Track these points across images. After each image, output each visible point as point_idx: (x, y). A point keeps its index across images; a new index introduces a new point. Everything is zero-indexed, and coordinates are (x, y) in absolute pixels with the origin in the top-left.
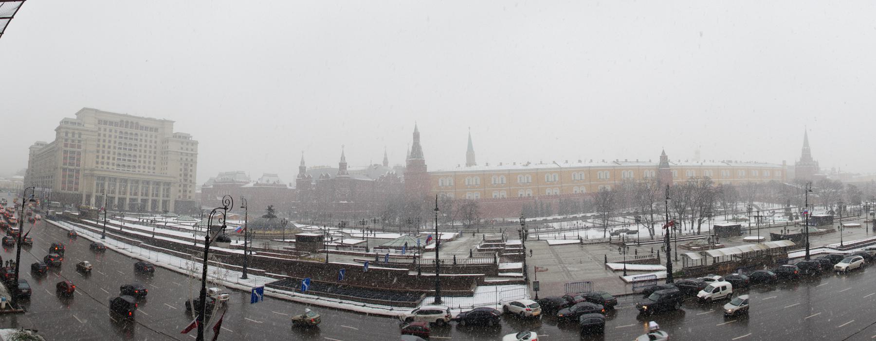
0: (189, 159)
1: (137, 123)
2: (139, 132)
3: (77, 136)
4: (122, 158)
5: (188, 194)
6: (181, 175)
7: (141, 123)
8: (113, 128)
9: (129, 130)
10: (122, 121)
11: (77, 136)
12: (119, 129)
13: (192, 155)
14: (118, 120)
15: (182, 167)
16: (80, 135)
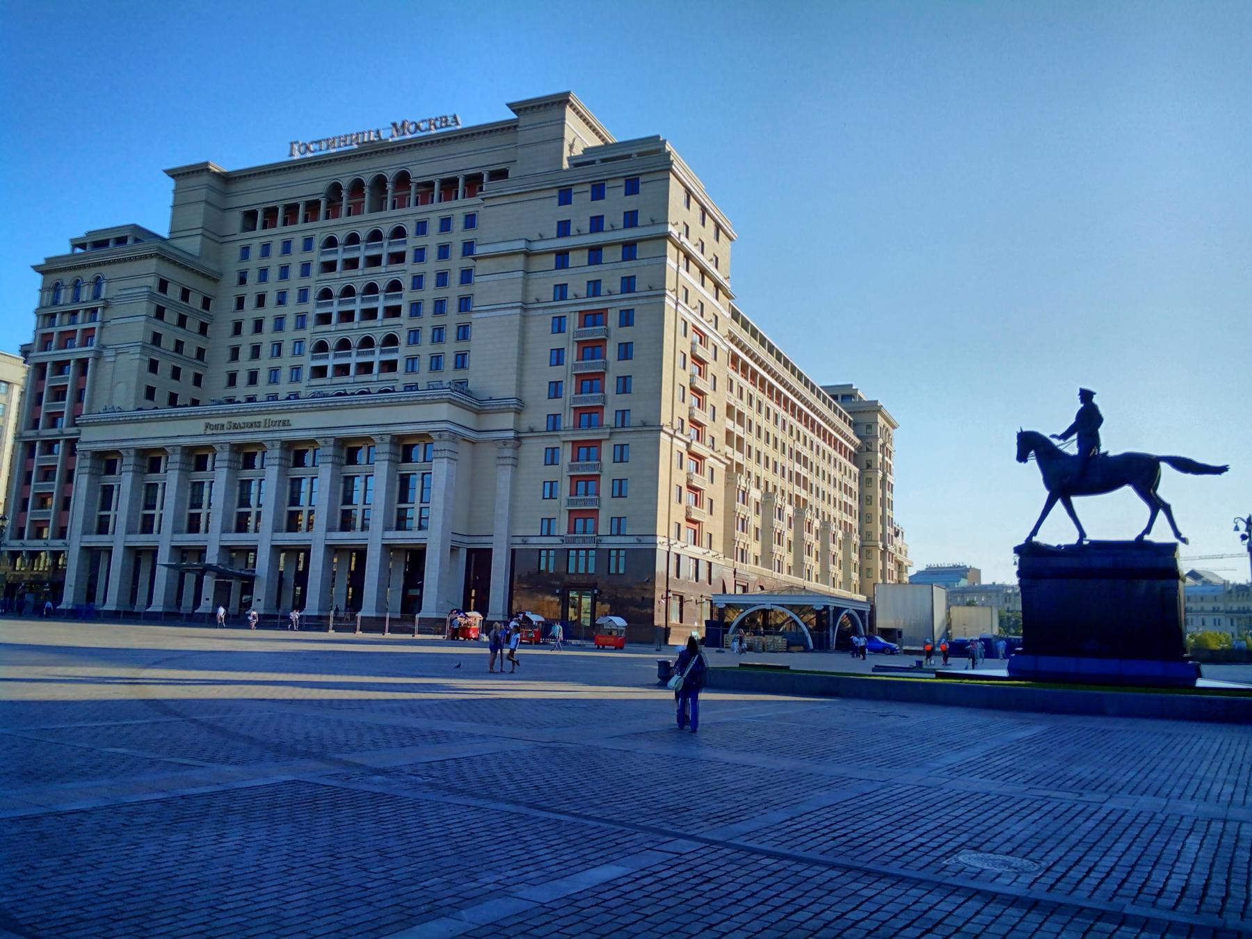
0: (611, 283)
1: (403, 179)
2: (408, 216)
3: (86, 293)
4: (330, 362)
5: (608, 508)
6: (555, 390)
7: (418, 172)
8: (298, 231)
9: (363, 224)
10: (336, 188)
11: (86, 293)
12: (321, 229)
13: (629, 250)
14: (314, 186)
15: (567, 342)
16: (97, 282)
